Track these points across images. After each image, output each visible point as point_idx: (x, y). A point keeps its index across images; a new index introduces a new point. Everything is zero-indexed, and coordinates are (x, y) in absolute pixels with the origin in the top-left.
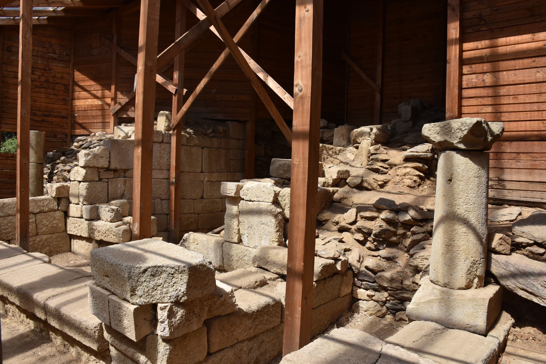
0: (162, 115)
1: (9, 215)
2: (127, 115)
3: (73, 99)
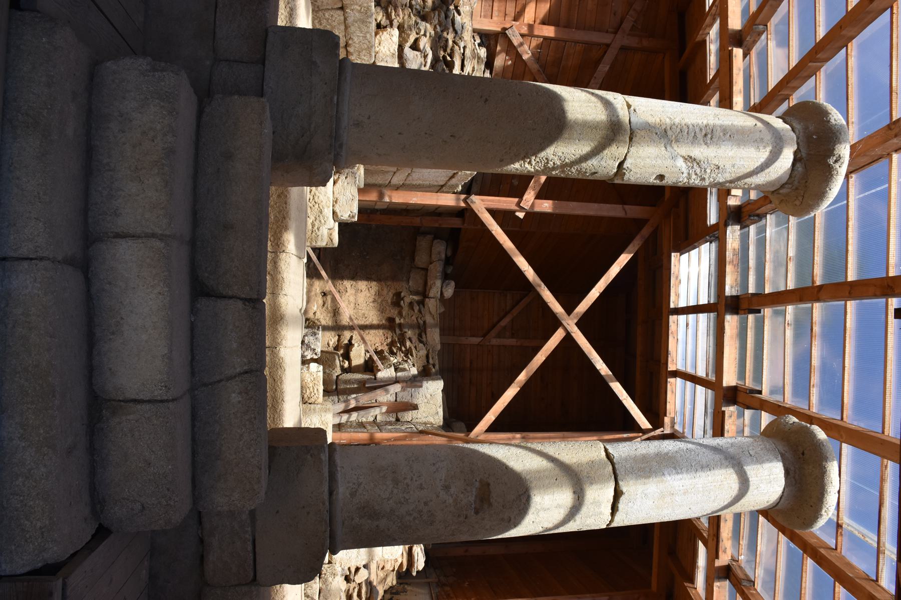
2: (500, 52)
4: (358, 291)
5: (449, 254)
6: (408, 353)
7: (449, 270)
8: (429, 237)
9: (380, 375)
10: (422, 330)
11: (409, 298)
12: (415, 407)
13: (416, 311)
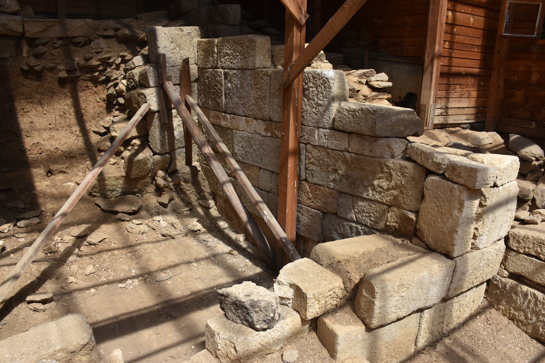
4: (33, 128)
6: (106, 63)
9: (155, 107)
10: (69, 43)
12: (186, 62)
13: (45, 49)
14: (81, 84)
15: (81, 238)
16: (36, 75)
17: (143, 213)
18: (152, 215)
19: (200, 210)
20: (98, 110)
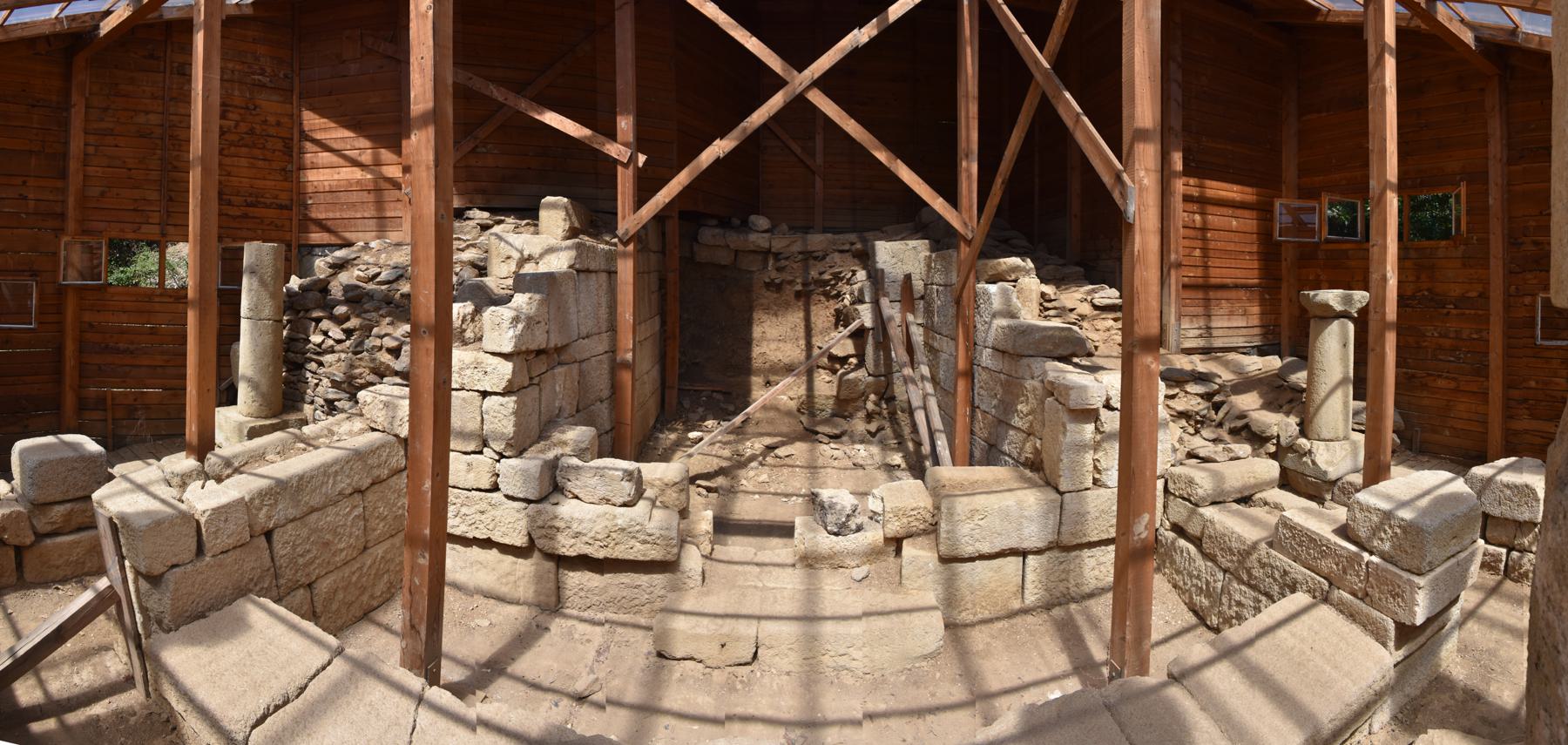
0: (554, 206)
1: (313, 510)
3: (302, 168)
4: (763, 338)
5: (714, 222)
6: (837, 277)
7: (736, 222)
8: (696, 248)
9: (868, 323)
10: (809, 257)
11: (772, 274)
12: (908, 277)
14: (815, 297)
15: (770, 448)
16: (777, 287)
17: (845, 438)
18: (854, 442)
19: (910, 445)
20: (827, 325)
